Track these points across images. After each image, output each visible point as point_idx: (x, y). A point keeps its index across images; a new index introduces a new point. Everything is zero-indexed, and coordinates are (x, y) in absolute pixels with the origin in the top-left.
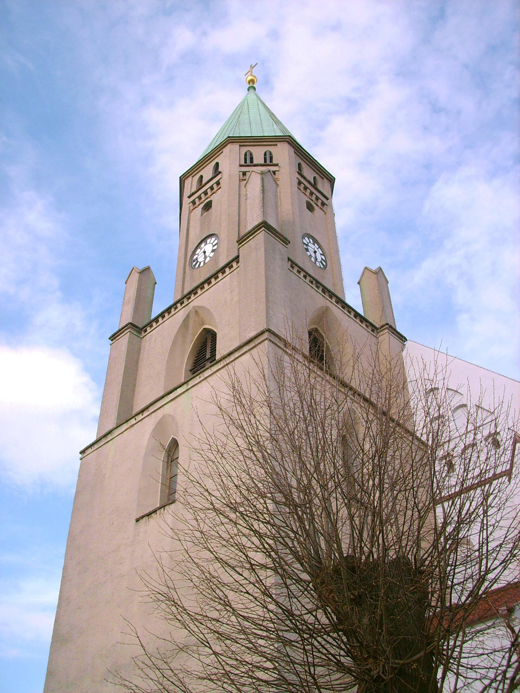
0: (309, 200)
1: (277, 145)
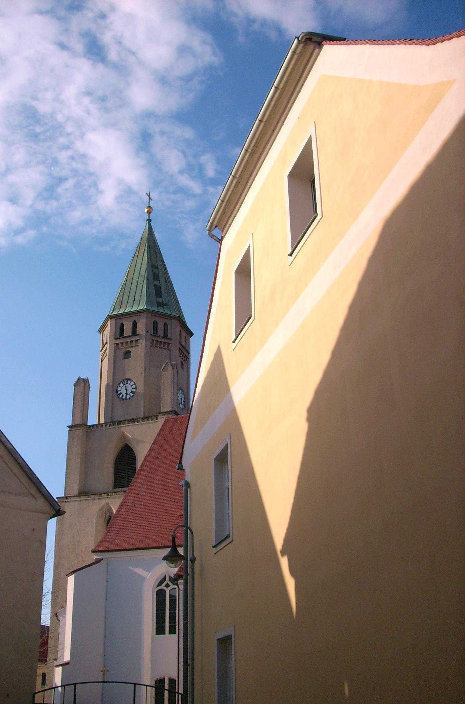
0: (182, 360)
1: (171, 320)
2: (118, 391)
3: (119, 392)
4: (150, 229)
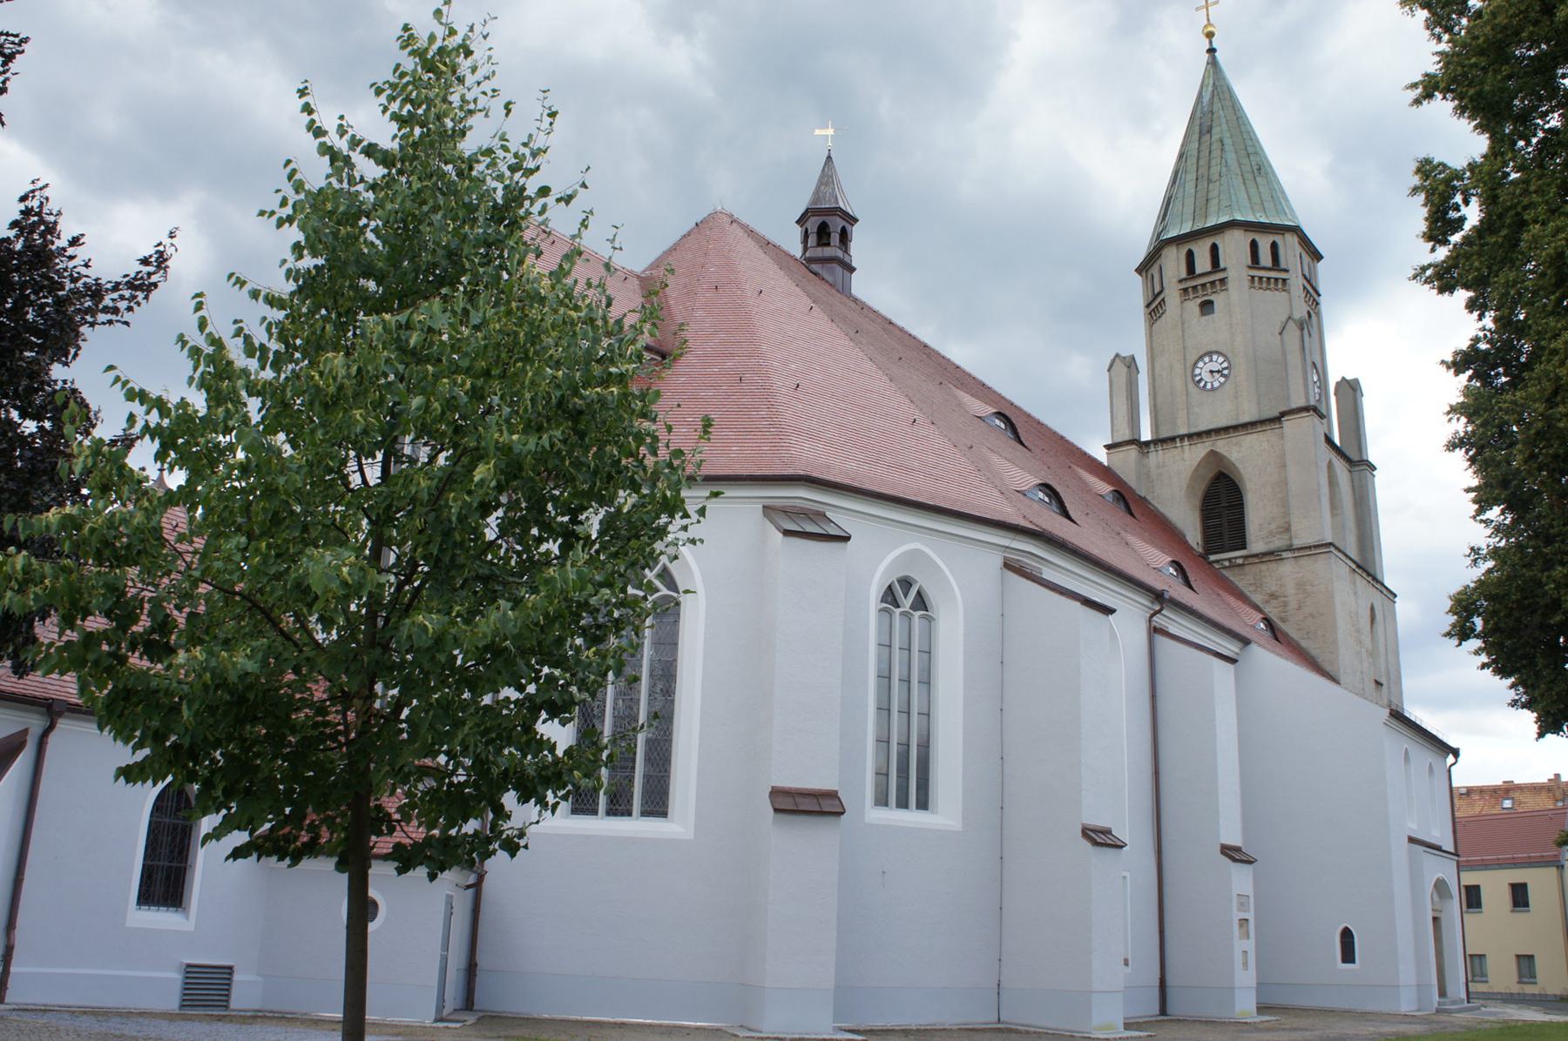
2: (1196, 376)
3: (1197, 378)
4: (1213, 63)
